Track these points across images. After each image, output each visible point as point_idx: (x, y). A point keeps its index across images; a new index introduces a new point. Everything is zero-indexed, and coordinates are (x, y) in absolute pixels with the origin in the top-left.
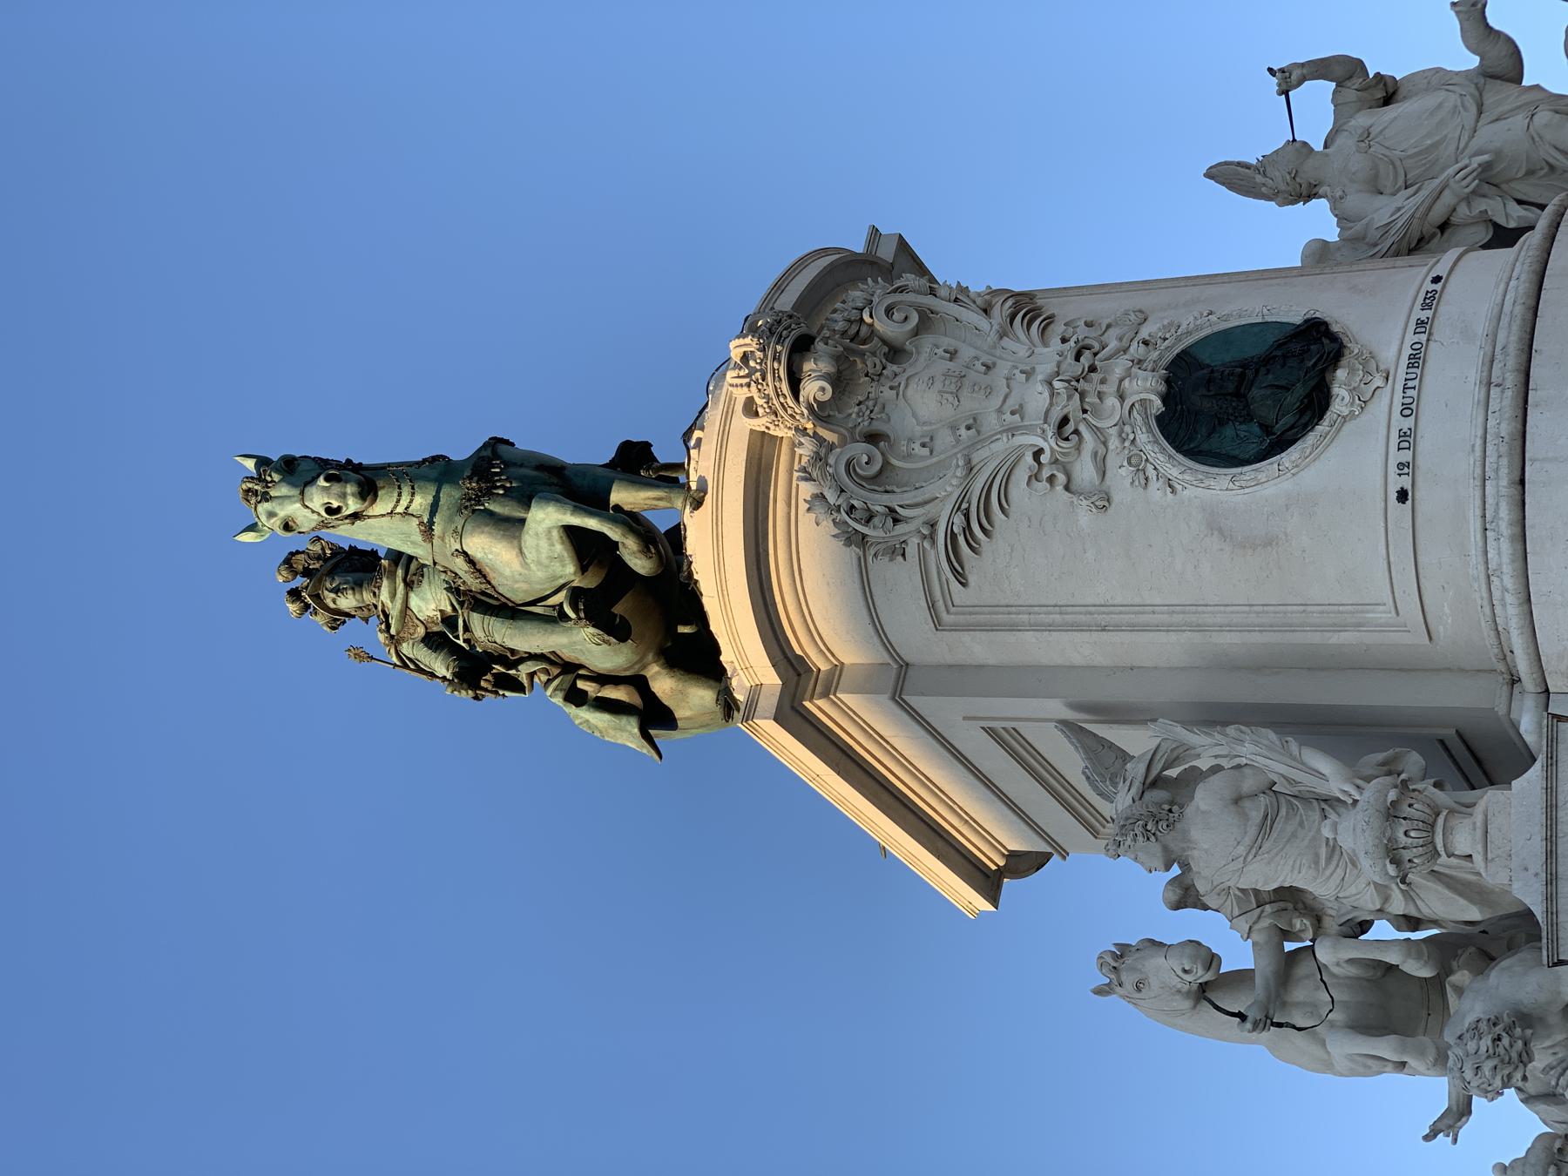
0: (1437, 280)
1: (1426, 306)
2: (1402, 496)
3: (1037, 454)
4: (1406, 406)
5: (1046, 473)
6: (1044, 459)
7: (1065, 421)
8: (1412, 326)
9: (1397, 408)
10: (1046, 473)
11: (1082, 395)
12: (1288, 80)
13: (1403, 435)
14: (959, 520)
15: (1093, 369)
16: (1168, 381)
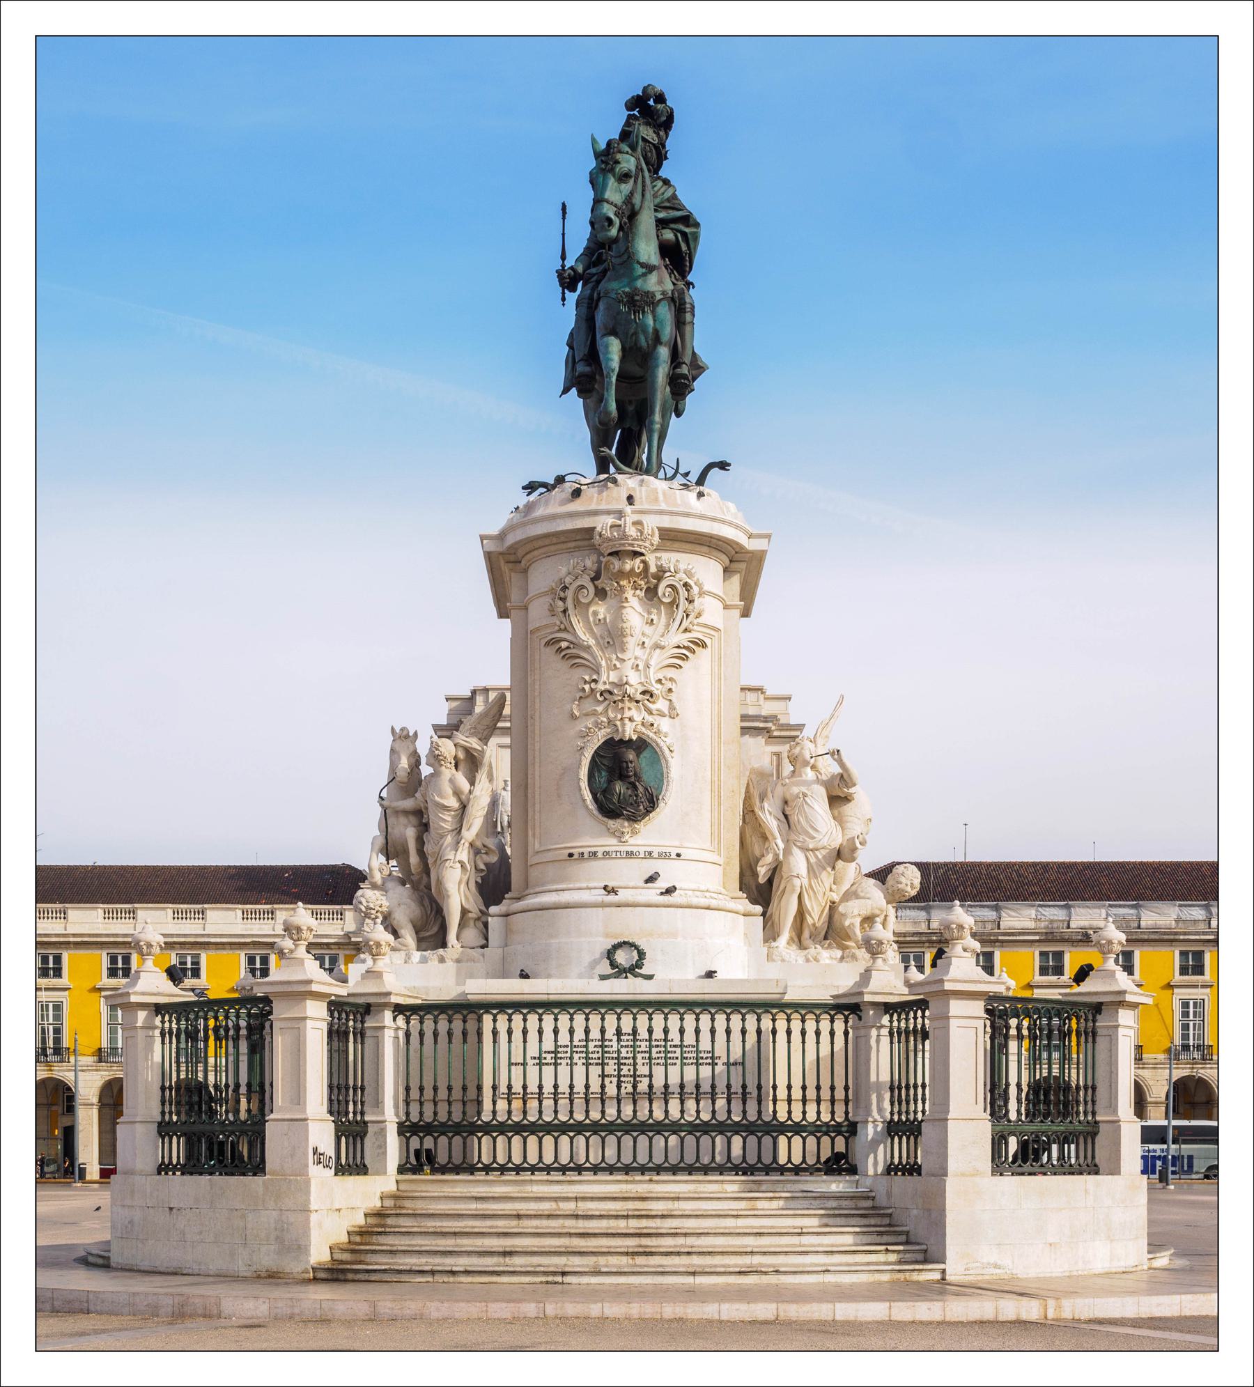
0: (678, 855)
1: (660, 854)
2: (571, 855)
3: (595, 681)
4: (608, 853)
5: (587, 687)
6: (593, 685)
7: (611, 693)
8: (649, 849)
9: (607, 849)
10: (587, 687)
11: (622, 701)
12: (836, 754)
13: (595, 853)
14: (564, 644)
15: (637, 702)
16: (630, 740)
